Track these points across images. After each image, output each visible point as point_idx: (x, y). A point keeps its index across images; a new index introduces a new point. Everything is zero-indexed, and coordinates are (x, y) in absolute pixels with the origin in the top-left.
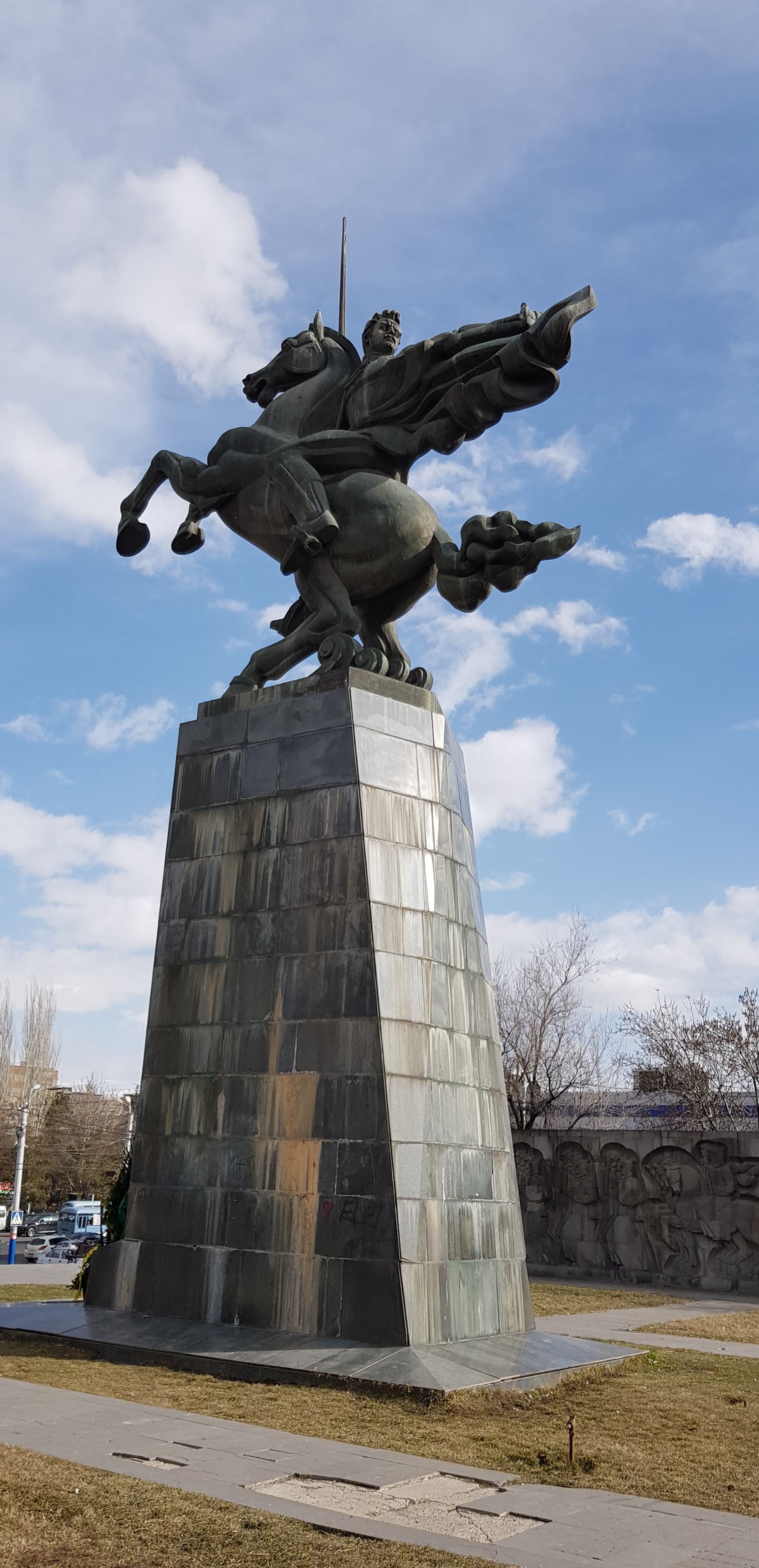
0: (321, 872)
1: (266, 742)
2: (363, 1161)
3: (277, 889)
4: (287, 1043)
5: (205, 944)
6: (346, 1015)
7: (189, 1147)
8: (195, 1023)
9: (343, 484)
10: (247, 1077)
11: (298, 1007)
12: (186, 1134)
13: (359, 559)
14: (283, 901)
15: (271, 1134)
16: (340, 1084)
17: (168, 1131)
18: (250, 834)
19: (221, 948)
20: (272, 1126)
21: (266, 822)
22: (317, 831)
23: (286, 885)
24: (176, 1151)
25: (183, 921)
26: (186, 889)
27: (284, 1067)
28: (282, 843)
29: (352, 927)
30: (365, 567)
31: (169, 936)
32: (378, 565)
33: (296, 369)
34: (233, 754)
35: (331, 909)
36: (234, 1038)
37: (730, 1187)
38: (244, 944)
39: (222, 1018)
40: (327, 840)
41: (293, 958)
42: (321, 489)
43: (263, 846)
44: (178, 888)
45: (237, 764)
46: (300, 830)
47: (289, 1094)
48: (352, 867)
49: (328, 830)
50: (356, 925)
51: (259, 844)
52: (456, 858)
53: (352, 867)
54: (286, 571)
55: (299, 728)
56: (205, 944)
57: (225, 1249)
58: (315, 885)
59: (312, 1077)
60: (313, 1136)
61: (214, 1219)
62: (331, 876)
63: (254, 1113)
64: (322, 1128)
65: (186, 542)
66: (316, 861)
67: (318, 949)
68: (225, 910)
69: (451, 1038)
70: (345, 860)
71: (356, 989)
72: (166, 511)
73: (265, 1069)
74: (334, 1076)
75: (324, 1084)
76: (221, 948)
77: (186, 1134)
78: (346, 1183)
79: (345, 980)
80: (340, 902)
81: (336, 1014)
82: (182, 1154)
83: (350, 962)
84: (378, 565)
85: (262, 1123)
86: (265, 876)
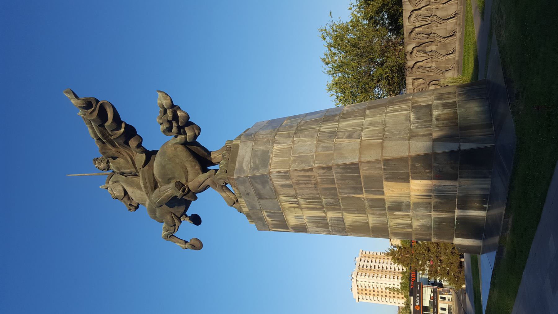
0: (305, 184)
1: (260, 204)
2: (418, 165)
3: (313, 198)
5: (338, 220)
6: (359, 173)
7: (416, 224)
8: (368, 223)
9: (160, 180)
10: (387, 206)
11: (358, 189)
12: (411, 224)
13: (186, 172)
14: (318, 196)
15: (409, 197)
16: (387, 175)
17: (410, 230)
18: (294, 207)
19: (338, 215)
20: (406, 197)
21: (290, 202)
22: (290, 186)
23: (312, 195)
24: (418, 227)
25: (330, 227)
27: (383, 193)
28: (295, 197)
29: (325, 173)
30: (189, 169)
31: (336, 232)
32: (188, 166)
33: (123, 194)
34: (266, 214)
35: (319, 180)
36: (372, 210)
38: (335, 207)
39: (366, 214)
41: (339, 192)
42: (163, 188)
43: (297, 202)
44: (318, 229)
45: (269, 212)
47: (392, 191)
48: (302, 173)
49: (289, 182)
50: (323, 171)
51: (298, 204)
52: (295, 128)
53: (302, 173)
54: (196, 198)
55: (252, 192)
56: (338, 220)
57: (457, 211)
58: (310, 185)
60: (409, 182)
61: (444, 215)
62: (306, 181)
63: (401, 202)
64: (405, 179)
65: (196, 220)
66: (301, 186)
68: (324, 214)
69: (366, 129)
70: (299, 176)
71: (349, 170)
72: (186, 229)
73: (384, 200)
75: (387, 179)
76: (338, 215)
77: (411, 224)
78: (428, 171)
79: (346, 174)
81: (359, 177)
82: (419, 226)
83: (338, 173)
84: (188, 166)
85: (405, 200)
86: (309, 202)
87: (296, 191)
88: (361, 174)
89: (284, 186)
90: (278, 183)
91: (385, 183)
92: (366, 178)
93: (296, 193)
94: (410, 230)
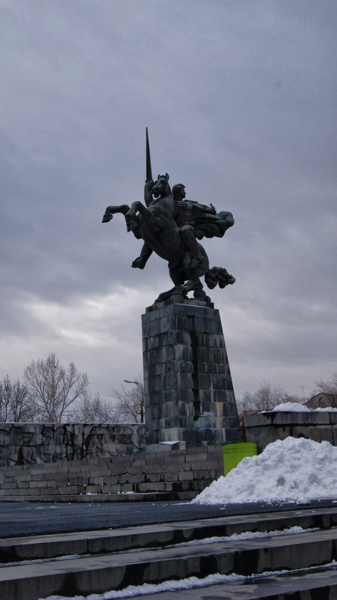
4: (215, 396)
11: (216, 387)
17: (188, 415)
23: (210, 356)
26: (183, 352)
35: (221, 365)
37: (22, 443)
40: (218, 347)
46: (211, 343)
48: (225, 356)
49: (218, 345)
59: (222, 403)
67: (219, 373)
70: (223, 354)
74: (226, 403)
75: (224, 405)
80: (223, 363)
87: (213, 347)
88: (227, 391)
89: (215, 341)
90: (217, 337)
91: (222, 403)
92: (224, 393)
93: (210, 347)
94: (188, 415)
